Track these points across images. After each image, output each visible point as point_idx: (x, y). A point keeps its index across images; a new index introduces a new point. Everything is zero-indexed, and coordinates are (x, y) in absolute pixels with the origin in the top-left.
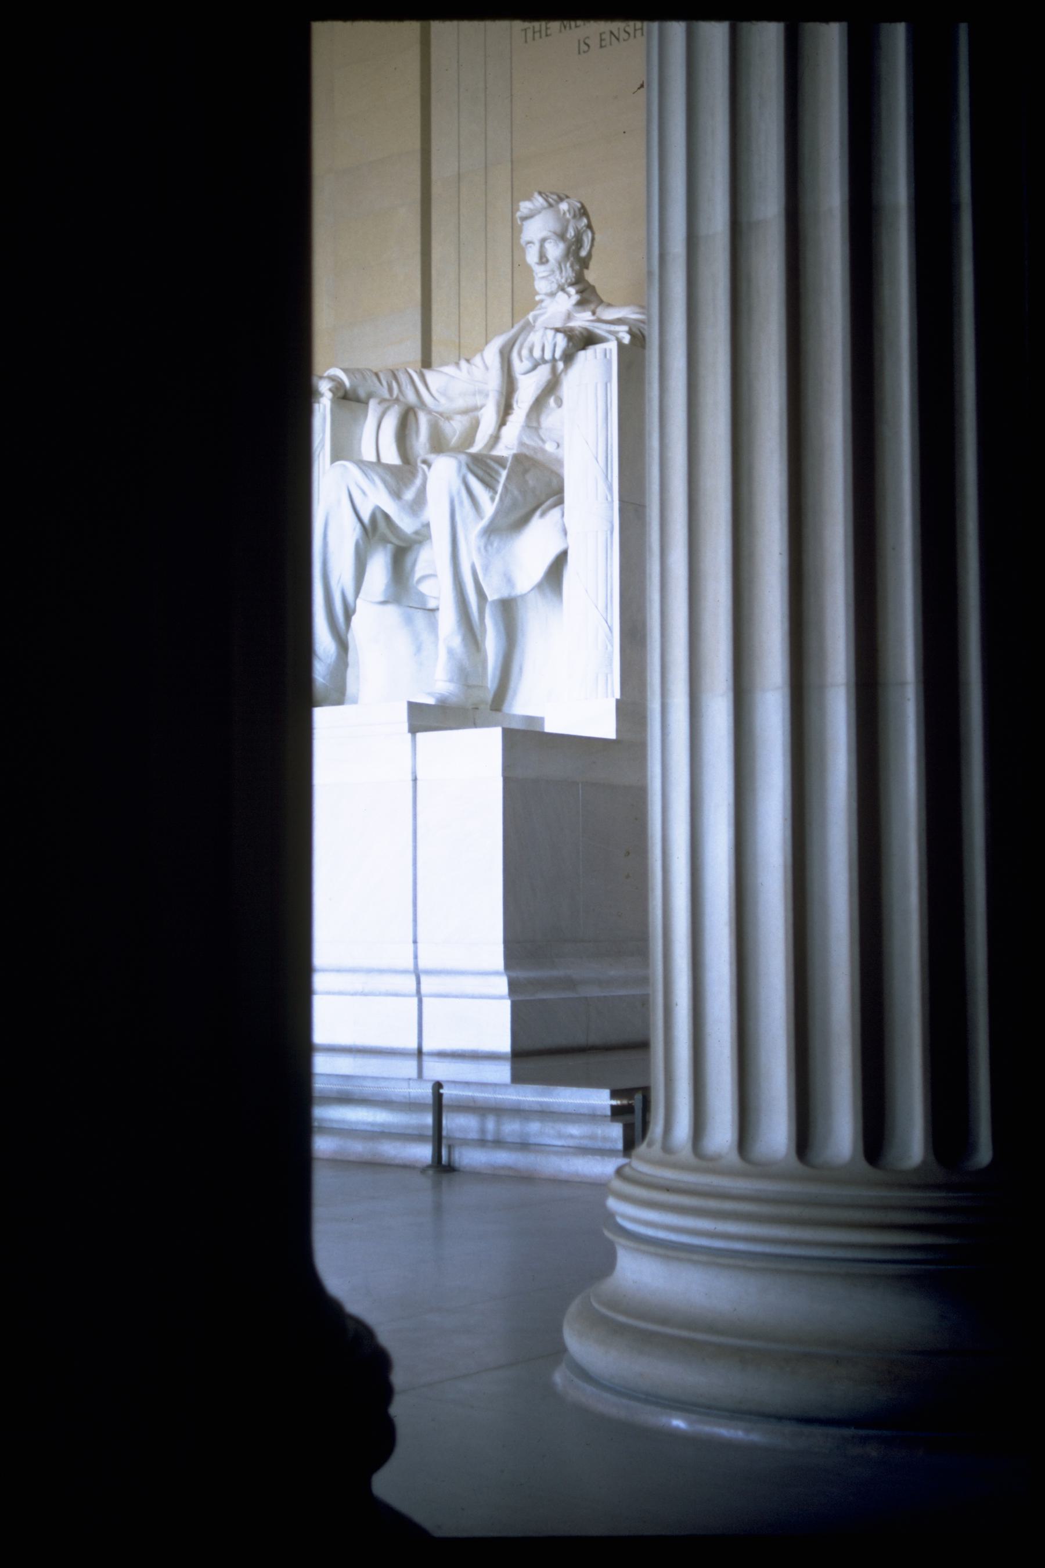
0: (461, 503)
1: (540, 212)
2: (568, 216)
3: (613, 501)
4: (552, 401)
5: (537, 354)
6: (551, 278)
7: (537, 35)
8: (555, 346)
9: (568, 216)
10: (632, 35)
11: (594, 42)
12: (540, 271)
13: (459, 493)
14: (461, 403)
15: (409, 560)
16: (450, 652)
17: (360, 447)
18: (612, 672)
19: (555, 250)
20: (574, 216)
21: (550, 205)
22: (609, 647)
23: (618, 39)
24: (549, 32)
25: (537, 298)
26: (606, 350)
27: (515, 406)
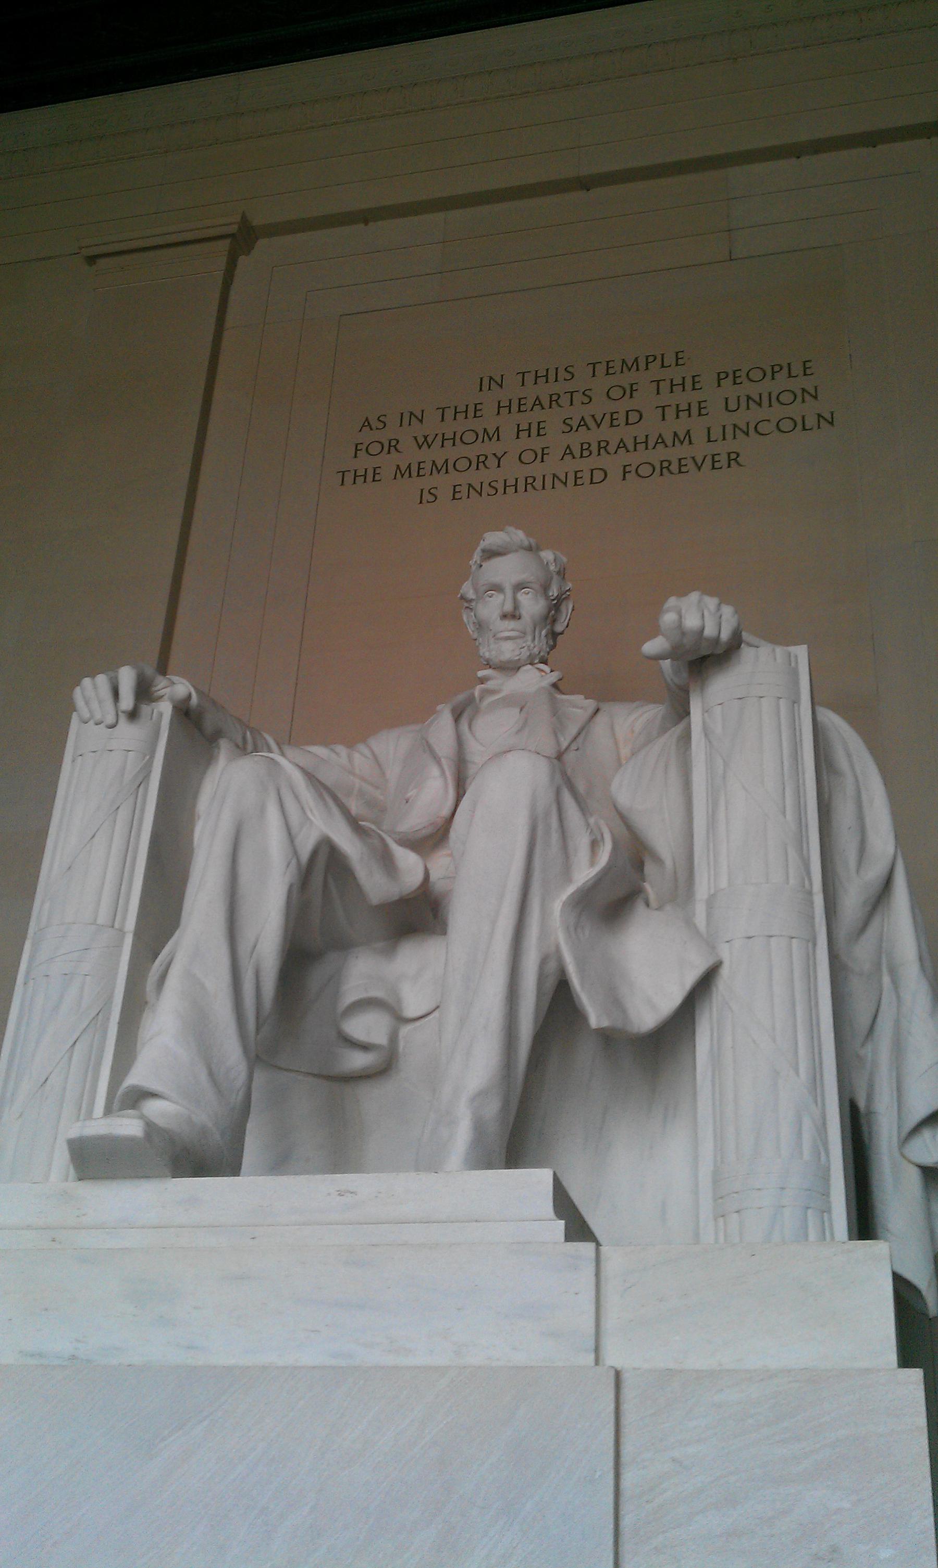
1: (516, 551)
2: (552, 568)
3: (810, 893)
6: (518, 641)
8: (721, 617)
9: (552, 568)
10: (501, 490)
11: (445, 493)
15: (317, 976)
16: (479, 1127)
17: (194, 806)
19: (532, 605)
20: (558, 573)
21: (530, 549)
24: (377, 478)
26: (790, 654)
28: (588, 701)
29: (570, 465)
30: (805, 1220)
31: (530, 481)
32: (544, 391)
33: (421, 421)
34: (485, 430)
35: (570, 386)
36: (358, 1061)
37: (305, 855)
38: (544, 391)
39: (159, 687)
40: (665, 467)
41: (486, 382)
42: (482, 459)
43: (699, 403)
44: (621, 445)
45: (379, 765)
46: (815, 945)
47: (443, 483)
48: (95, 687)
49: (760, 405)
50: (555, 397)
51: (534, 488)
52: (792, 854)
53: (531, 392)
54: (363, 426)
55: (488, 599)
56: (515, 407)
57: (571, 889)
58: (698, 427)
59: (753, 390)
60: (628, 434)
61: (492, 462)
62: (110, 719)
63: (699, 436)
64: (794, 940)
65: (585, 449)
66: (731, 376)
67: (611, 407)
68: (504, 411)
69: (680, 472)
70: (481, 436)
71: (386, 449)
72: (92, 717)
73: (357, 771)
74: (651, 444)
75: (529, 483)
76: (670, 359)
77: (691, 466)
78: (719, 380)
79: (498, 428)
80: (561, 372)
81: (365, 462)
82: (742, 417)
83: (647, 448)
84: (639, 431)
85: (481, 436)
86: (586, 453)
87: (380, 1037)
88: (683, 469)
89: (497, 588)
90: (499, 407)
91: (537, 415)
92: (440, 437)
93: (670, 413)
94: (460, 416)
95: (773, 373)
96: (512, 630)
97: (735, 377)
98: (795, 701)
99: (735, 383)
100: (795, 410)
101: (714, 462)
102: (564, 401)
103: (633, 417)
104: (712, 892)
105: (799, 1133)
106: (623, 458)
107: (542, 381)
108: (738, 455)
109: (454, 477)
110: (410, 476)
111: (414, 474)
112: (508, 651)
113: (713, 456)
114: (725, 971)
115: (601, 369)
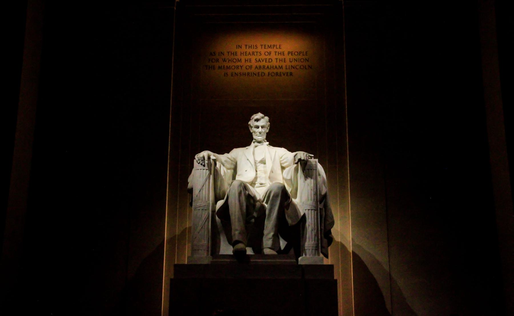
25: (254, 141)
32: (251, 50)
35: (257, 50)
38: (251, 50)
53: (249, 50)
61: (240, 68)
63: (284, 68)
65: (260, 67)
67: (266, 57)
76: (278, 47)
77: (282, 75)
80: (255, 47)
93: (278, 60)
102: (255, 54)
103: (270, 60)
112: (260, 138)
115: (263, 47)
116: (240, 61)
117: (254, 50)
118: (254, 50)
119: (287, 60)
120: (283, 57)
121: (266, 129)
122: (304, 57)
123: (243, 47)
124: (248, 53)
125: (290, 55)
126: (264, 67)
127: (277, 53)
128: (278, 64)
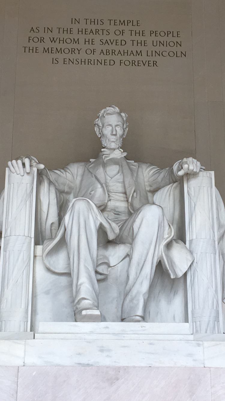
0: (161, 228)
2: (125, 119)
3: (215, 241)
4: (135, 194)
5: (191, 168)
7: (31, 51)
9: (125, 119)
10: (80, 63)
11: (61, 61)
12: (113, 138)
13: (161, 223)
14: (61, 188)
18: (219, 322)
19: (119, 131)
22: (218, 308)
23: (73, 63)
25: (102, 150)
27: (109, 193)
28: (135, 163)
29: (102, 57)
30: (215, 324)
31: (90, 61)
32: (94, 27)
33: (52, 32)
34: (74, 39)
36: (100, 277)
37: (97, 229)
38: (94, 27)
39: (32, 163)
40: (133, 63)
41: (74, 20)
42: (73, 50)
43: (144, 41)
44: (119, 52)
45: (73, 177)
46: (216, 254)
47: (61, 57)
48: (17, 163)
49: (163, 45)
50: (97, 31)
51: (91, 64)
52: (211, 230)
53: (90, 27)
54: (31, 30)
55: (107, 128)
56: (84, 31)
57: (166, 242)
58: (143, 49)
59: (162, 39)
60: (122, 48)
61: (77, 51)
62: (22, 174)
63: (144, 54)
64: (212, 254)
65: (108, 52)
66: (154, 33)
67: (116, 38)
68: (80, 33)
69: (138, 65)
70: (72, 42)
71: (40, 41)
72: (16, 172)
73: (68, 178)
74: (129, 54)
75: (89, 62)
76: (135, 23)
78: (151, 34)
79: (78, 39)
80: (99, 22)
81: (32, 45)
82: (158, 49)
83: (128, 55)
84: (125, 48)
85: (72, 42)
86: (108, 53)
87: (105, 272)
88: (139, 65)
89: (110, 125)
90: (78, 31)
91: (91, 36)
92: (58, 39)
93: (135, 43)
94: (65, 32)
95: (168, 34)
96: (114, 139)
97: (156, 34)
98: (212, 187)
99: (156, 36)
100: (174, 49)
101: (149, 63)
102: (101, 32)
103: (123, 43)
104: (191, 239)
105: (213, 303)
106: (119, 57)
107: (93, 23)
108: (156, 63)
109: (64, 56)
110: (49, 53)
111: (50, 52)
112: (113, 145)
113: (149, 61)
114: (195, 261)
115: (112, 22)
116: (77, 41)
117: (99, 27)
118: (99, 27)
119: (149, 42)
120: (143, 39)
121: (122, 130)
122: (175, 39)
123: (83, 22)
124: (89, 31)
125: (153, 35)
126: (113, 52)
127: (133, 33)
128: (135, 49)
